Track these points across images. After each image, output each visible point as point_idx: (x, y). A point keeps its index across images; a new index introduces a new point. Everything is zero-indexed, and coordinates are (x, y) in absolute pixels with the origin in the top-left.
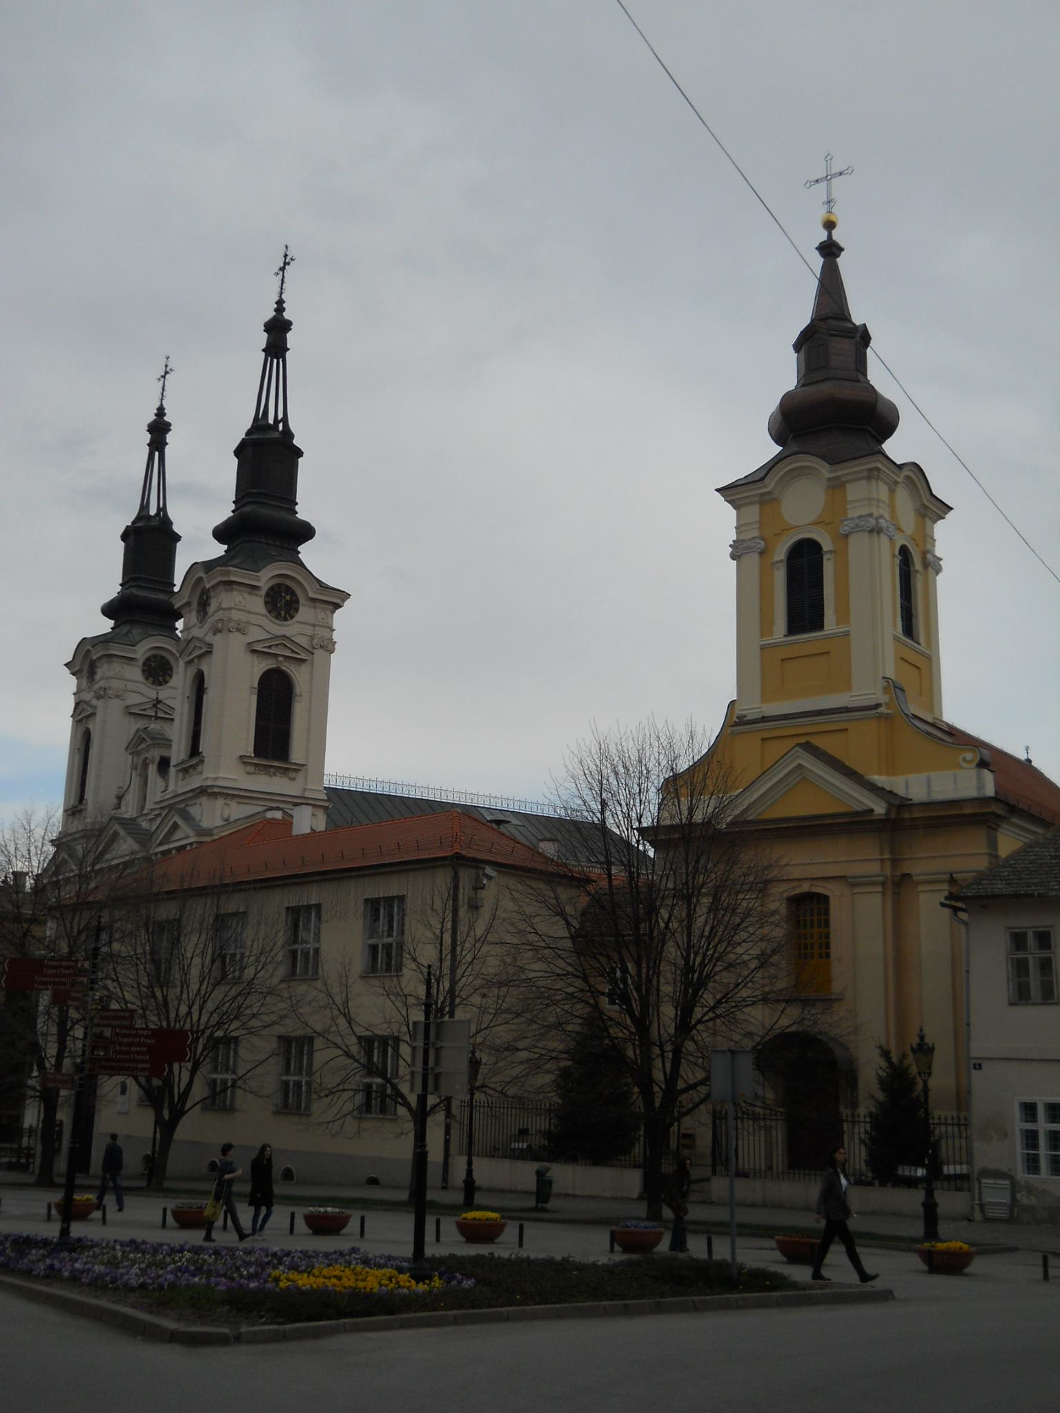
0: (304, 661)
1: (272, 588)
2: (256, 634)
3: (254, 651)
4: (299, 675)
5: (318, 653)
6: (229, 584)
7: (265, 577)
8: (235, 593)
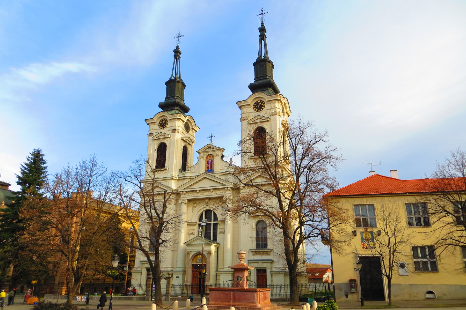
0: (268, 121)
2: (249, 118)
3: (251, 124)
4: (266, 126)
5: (273, 117)
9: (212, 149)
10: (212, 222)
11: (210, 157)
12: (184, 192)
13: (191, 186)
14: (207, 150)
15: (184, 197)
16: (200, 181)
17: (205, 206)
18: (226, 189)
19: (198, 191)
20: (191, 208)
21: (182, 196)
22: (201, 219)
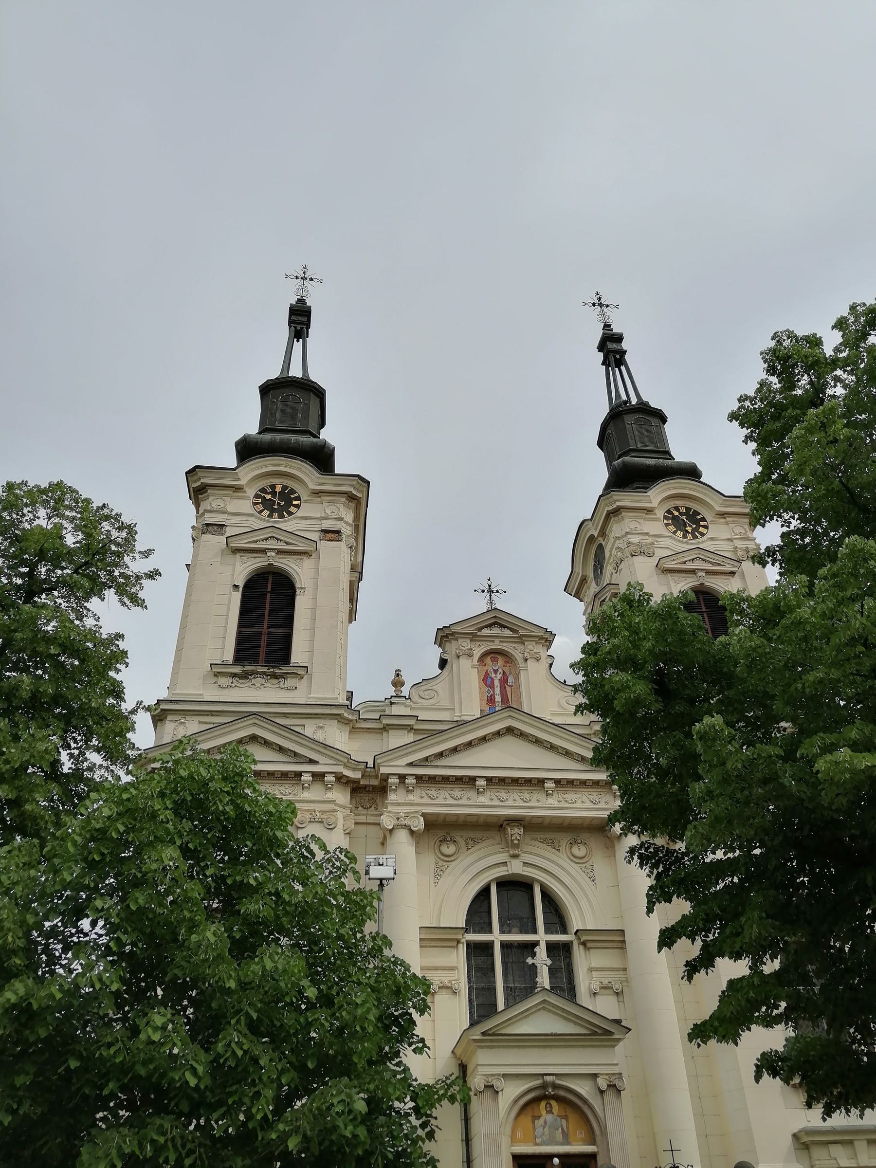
0: (733, 573)
1: (669, 512)
2: (660, 553)
6: (617, 511)
7: (657, 495)
8: (627, 521)
9: (507, 632)
10: (542, 937)
11: (494, 660)
12: (411, 781)
13: (441, 755)
14: (486, 631)
15: (406, 806)
16: (484, 739)
17: (503, 857)
19: (481, 783)
20: (430, 860)
21: (392, 797)
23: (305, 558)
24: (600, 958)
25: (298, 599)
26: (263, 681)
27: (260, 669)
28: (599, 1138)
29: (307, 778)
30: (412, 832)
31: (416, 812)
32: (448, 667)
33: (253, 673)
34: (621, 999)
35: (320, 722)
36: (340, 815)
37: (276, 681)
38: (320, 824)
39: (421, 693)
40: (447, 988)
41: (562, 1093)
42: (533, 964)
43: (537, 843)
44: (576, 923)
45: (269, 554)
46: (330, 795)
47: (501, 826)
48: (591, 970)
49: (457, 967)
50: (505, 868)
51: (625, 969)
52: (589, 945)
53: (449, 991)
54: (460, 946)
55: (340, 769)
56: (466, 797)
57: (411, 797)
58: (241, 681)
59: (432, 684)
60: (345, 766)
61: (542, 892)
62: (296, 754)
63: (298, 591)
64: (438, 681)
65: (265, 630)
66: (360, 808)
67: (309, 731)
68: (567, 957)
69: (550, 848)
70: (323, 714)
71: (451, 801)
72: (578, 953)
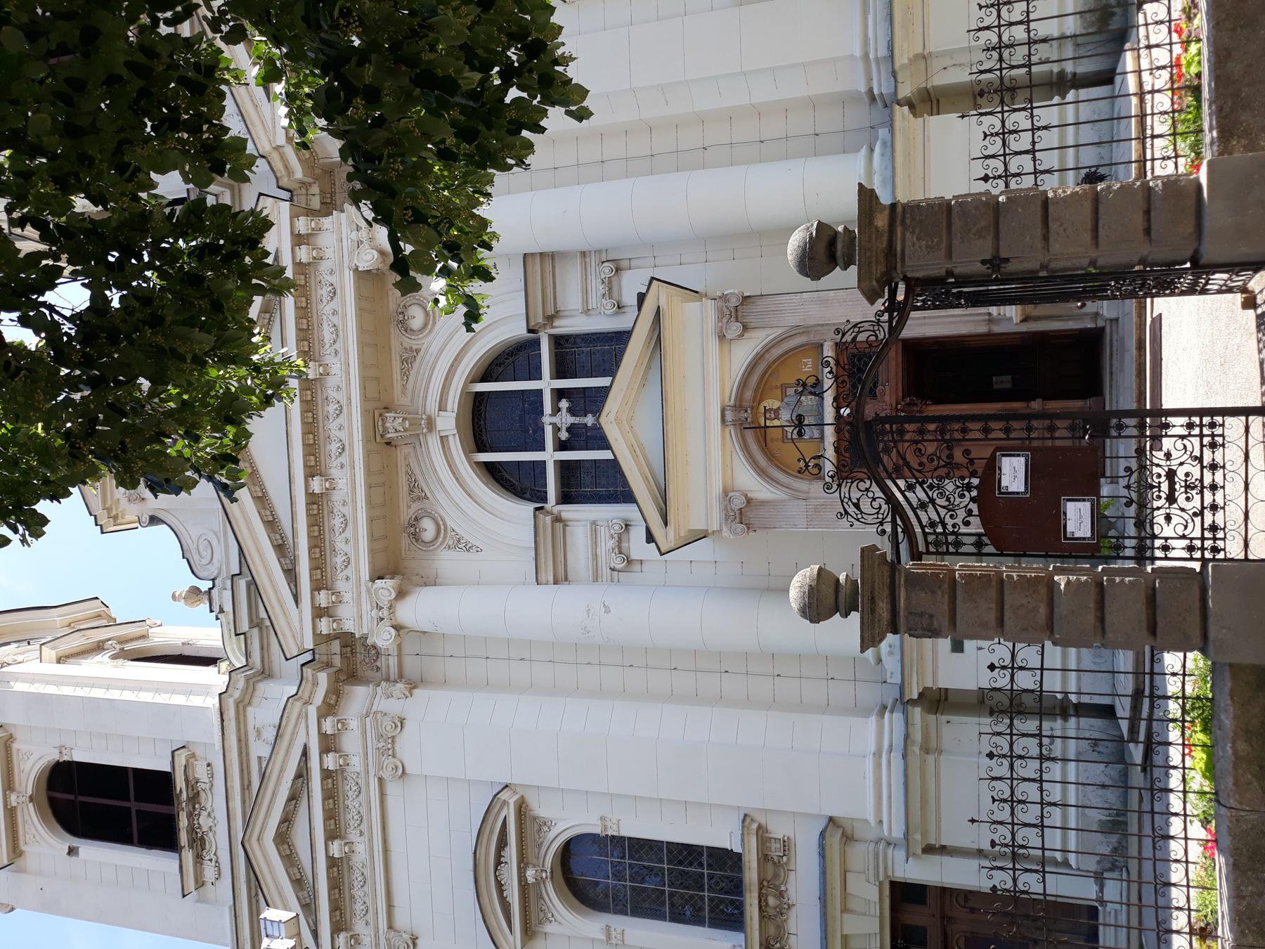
12: (323, 599)
15: (360, 606)
17: (434, 443)
18: (304, 254)
19: (317, 485)
21: (349, 626)
22: (517, 483)
23: (15, 746)
24: (570, 297)
25: (79, 757)
26: (204, 813)
27: (183, 822)
28: (814, 338)
29: (331, 761)
30: (401, 594)
31: (368, 591)
32: (161, 515)
33: (192, 830)
34: (625, 264)
35: (252, 735)
36: (382, 704)
37: (202, 795)
38: (397, 739)
39: (205, 561)
40: (620, 541)
41: (749, 394)
42: (568, 430)
43: (410, 385)
44: (517, 330)
45: (14, 804)
46: (354, 724)
47: (388, 444)
48: (586, 311)
49: (594, 523)
50: (451, 439)
51: (583, 254)
52: (550, 311)
53: (624, 537)
54: (564, 515)
55: (312, 711)
56: (342, 509)
57: (347, 597)
58: (207, 847)
59: (190, 542)
60: (308, 703)
61: (485, 378)
62: (299, 776)
63: (66, 758)
64: (183, 530)
65: (134, 805)
66: (378, 664)
67: (265, 751)
68: (575, 343)
69: (416, 365)
70: (239, 730)
71: (349, 533)
72: (566, 326)
